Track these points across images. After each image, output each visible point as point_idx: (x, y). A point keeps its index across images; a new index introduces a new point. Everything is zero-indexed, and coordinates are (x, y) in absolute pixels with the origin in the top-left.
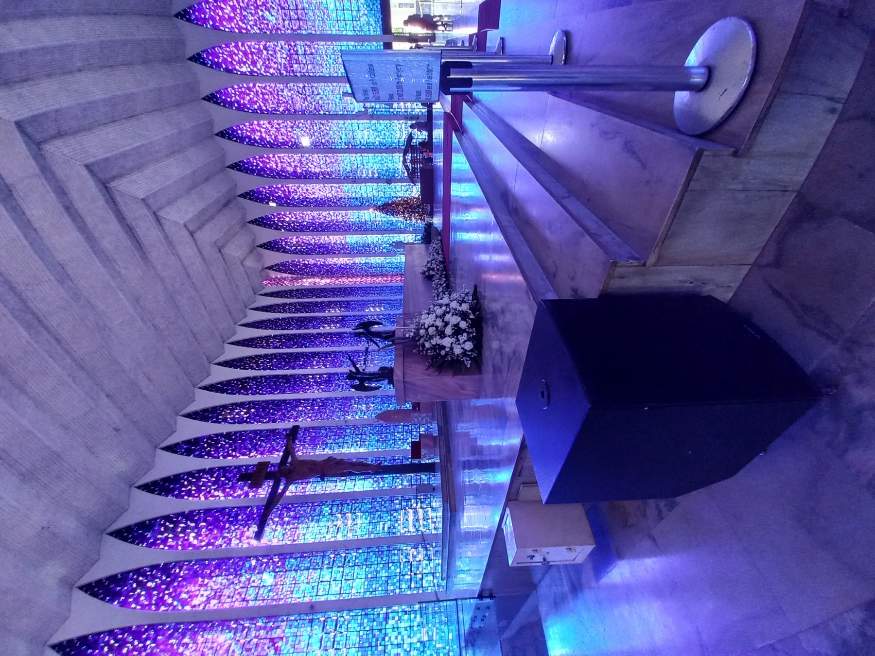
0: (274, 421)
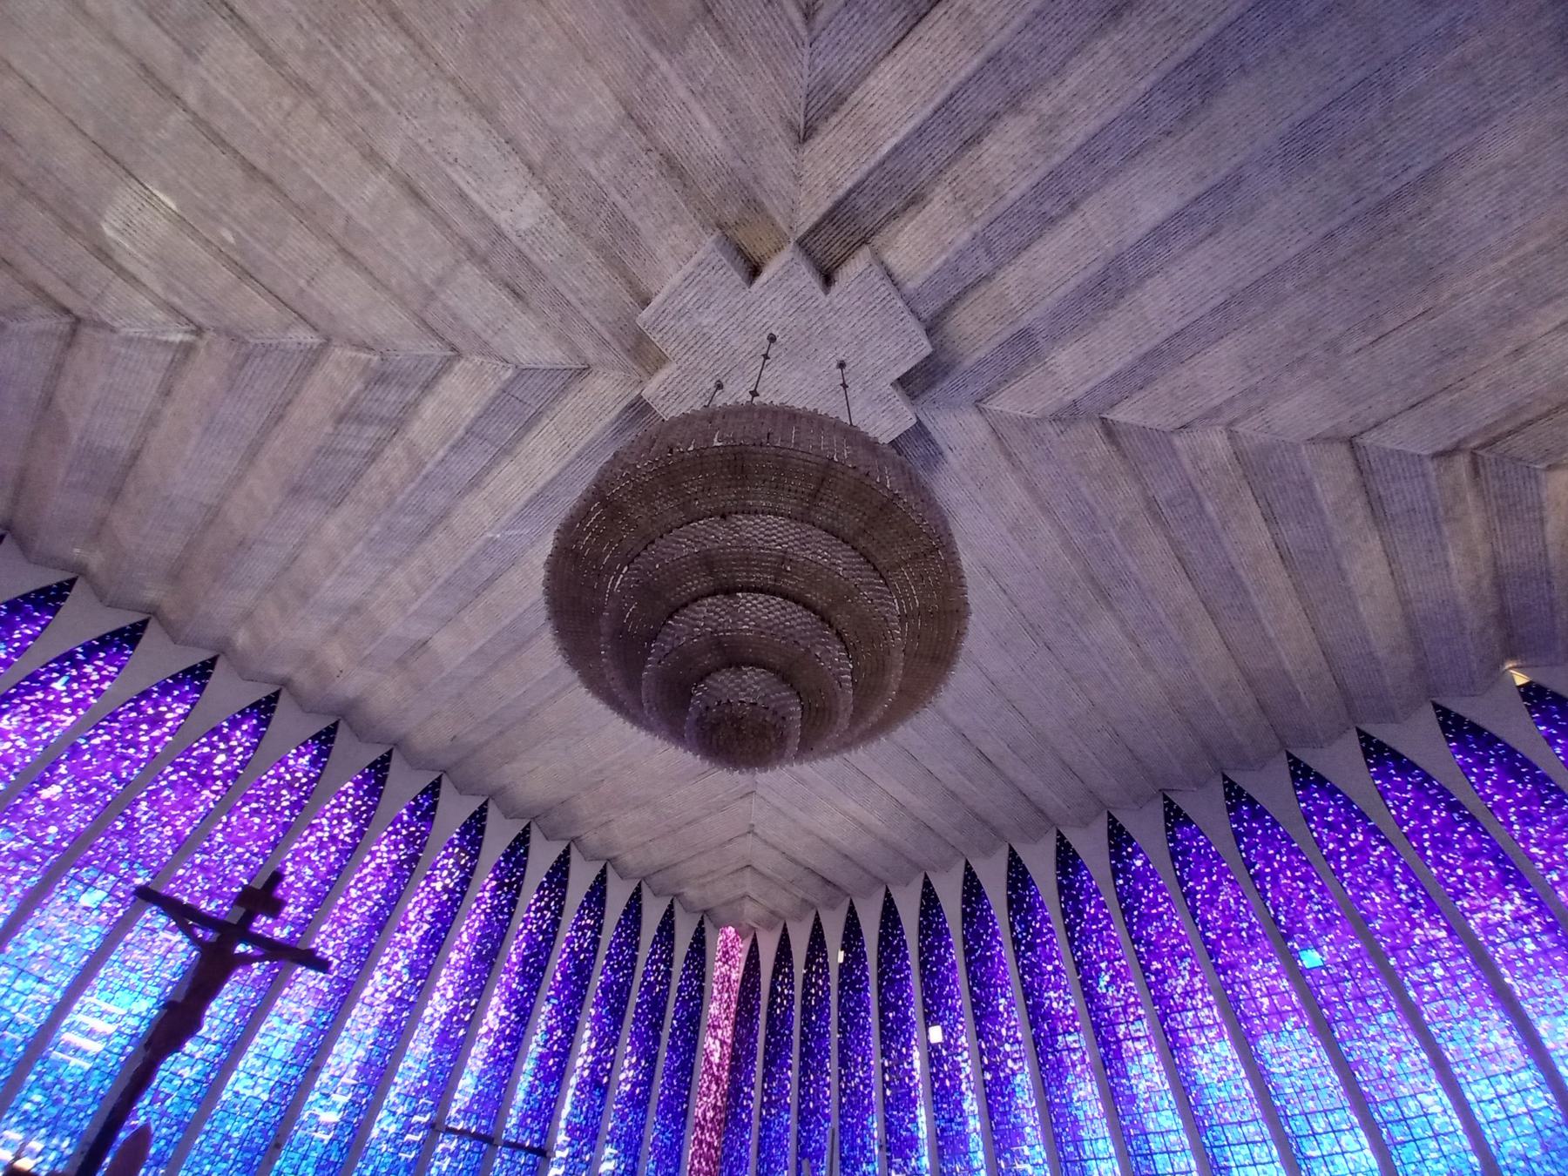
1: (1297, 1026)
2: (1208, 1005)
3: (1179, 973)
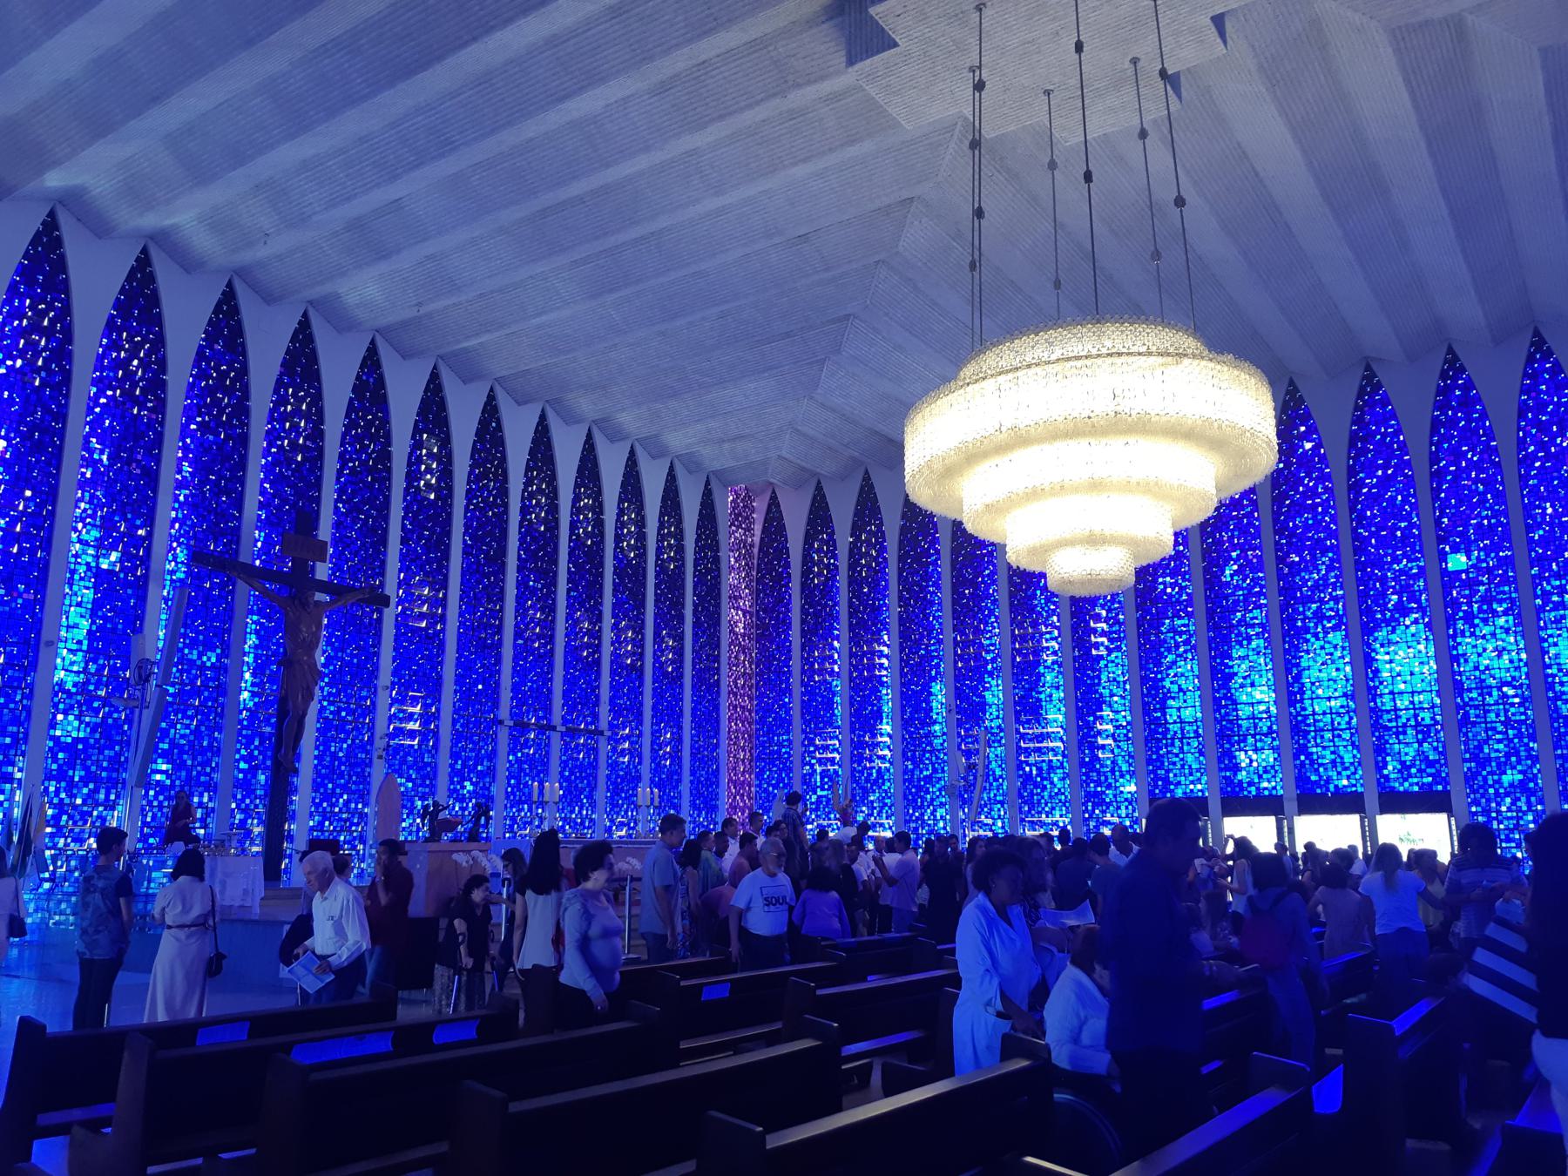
0: (404, 541)
1: (1416, 622)
2: (1336, 600)
3: (1316, 567)
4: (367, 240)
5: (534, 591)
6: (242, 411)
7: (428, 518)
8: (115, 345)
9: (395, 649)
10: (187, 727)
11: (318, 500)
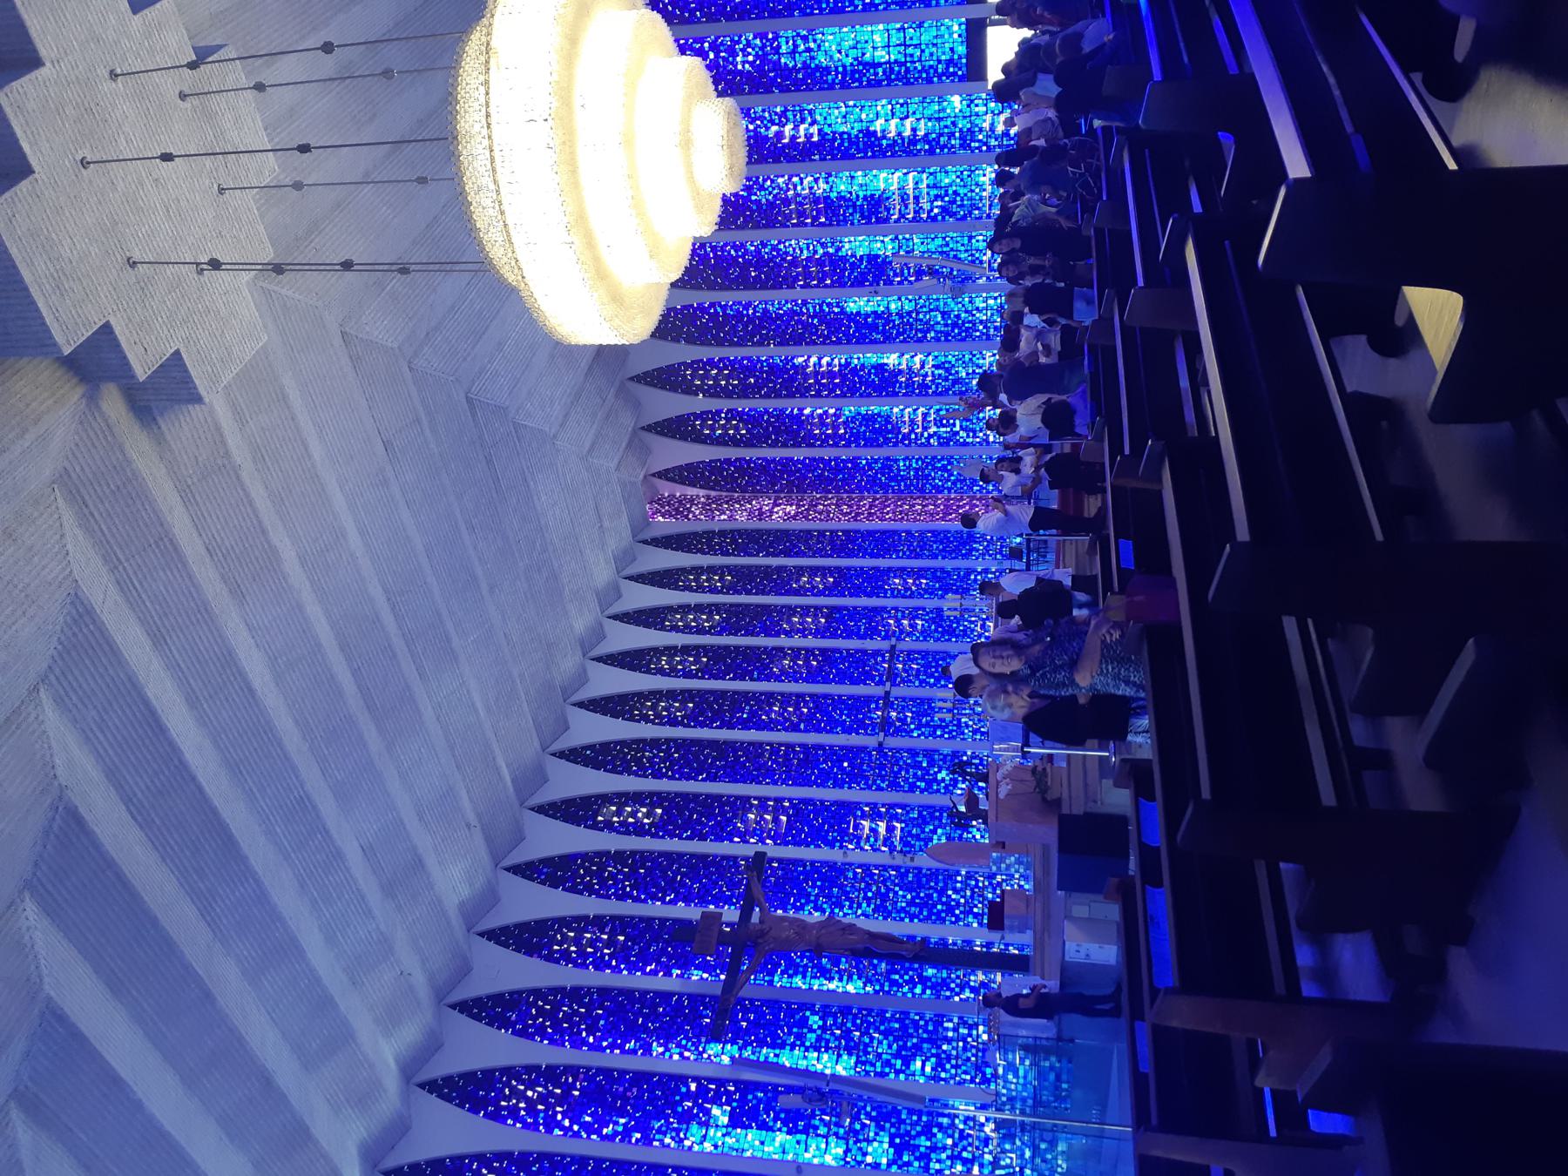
0: (703, 838)
4: (405, 876)
5: (752, 714)
6: (576, 994)
7: (678, 815)
8: (513, 1112)
9: (808, 845)
10: (880, 1042)
11: (663, 921)
